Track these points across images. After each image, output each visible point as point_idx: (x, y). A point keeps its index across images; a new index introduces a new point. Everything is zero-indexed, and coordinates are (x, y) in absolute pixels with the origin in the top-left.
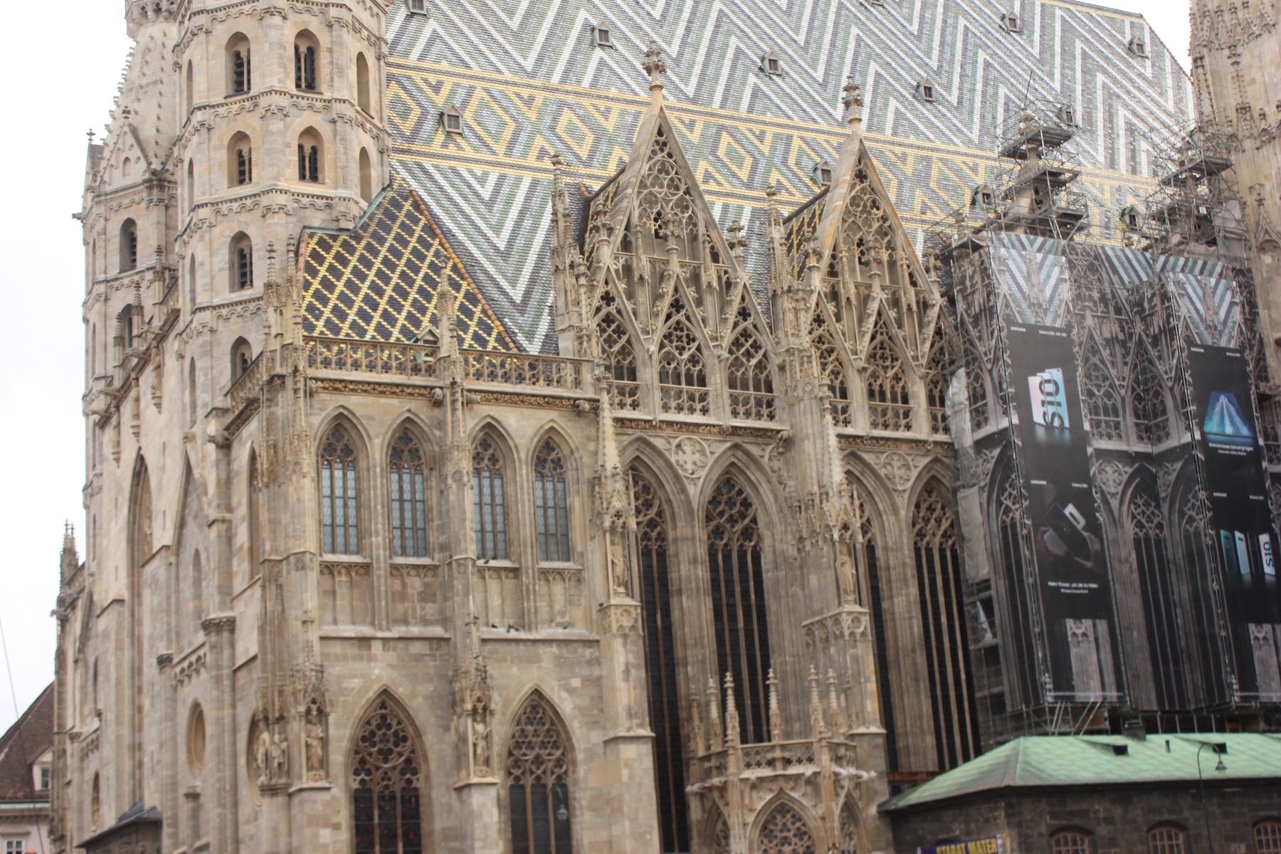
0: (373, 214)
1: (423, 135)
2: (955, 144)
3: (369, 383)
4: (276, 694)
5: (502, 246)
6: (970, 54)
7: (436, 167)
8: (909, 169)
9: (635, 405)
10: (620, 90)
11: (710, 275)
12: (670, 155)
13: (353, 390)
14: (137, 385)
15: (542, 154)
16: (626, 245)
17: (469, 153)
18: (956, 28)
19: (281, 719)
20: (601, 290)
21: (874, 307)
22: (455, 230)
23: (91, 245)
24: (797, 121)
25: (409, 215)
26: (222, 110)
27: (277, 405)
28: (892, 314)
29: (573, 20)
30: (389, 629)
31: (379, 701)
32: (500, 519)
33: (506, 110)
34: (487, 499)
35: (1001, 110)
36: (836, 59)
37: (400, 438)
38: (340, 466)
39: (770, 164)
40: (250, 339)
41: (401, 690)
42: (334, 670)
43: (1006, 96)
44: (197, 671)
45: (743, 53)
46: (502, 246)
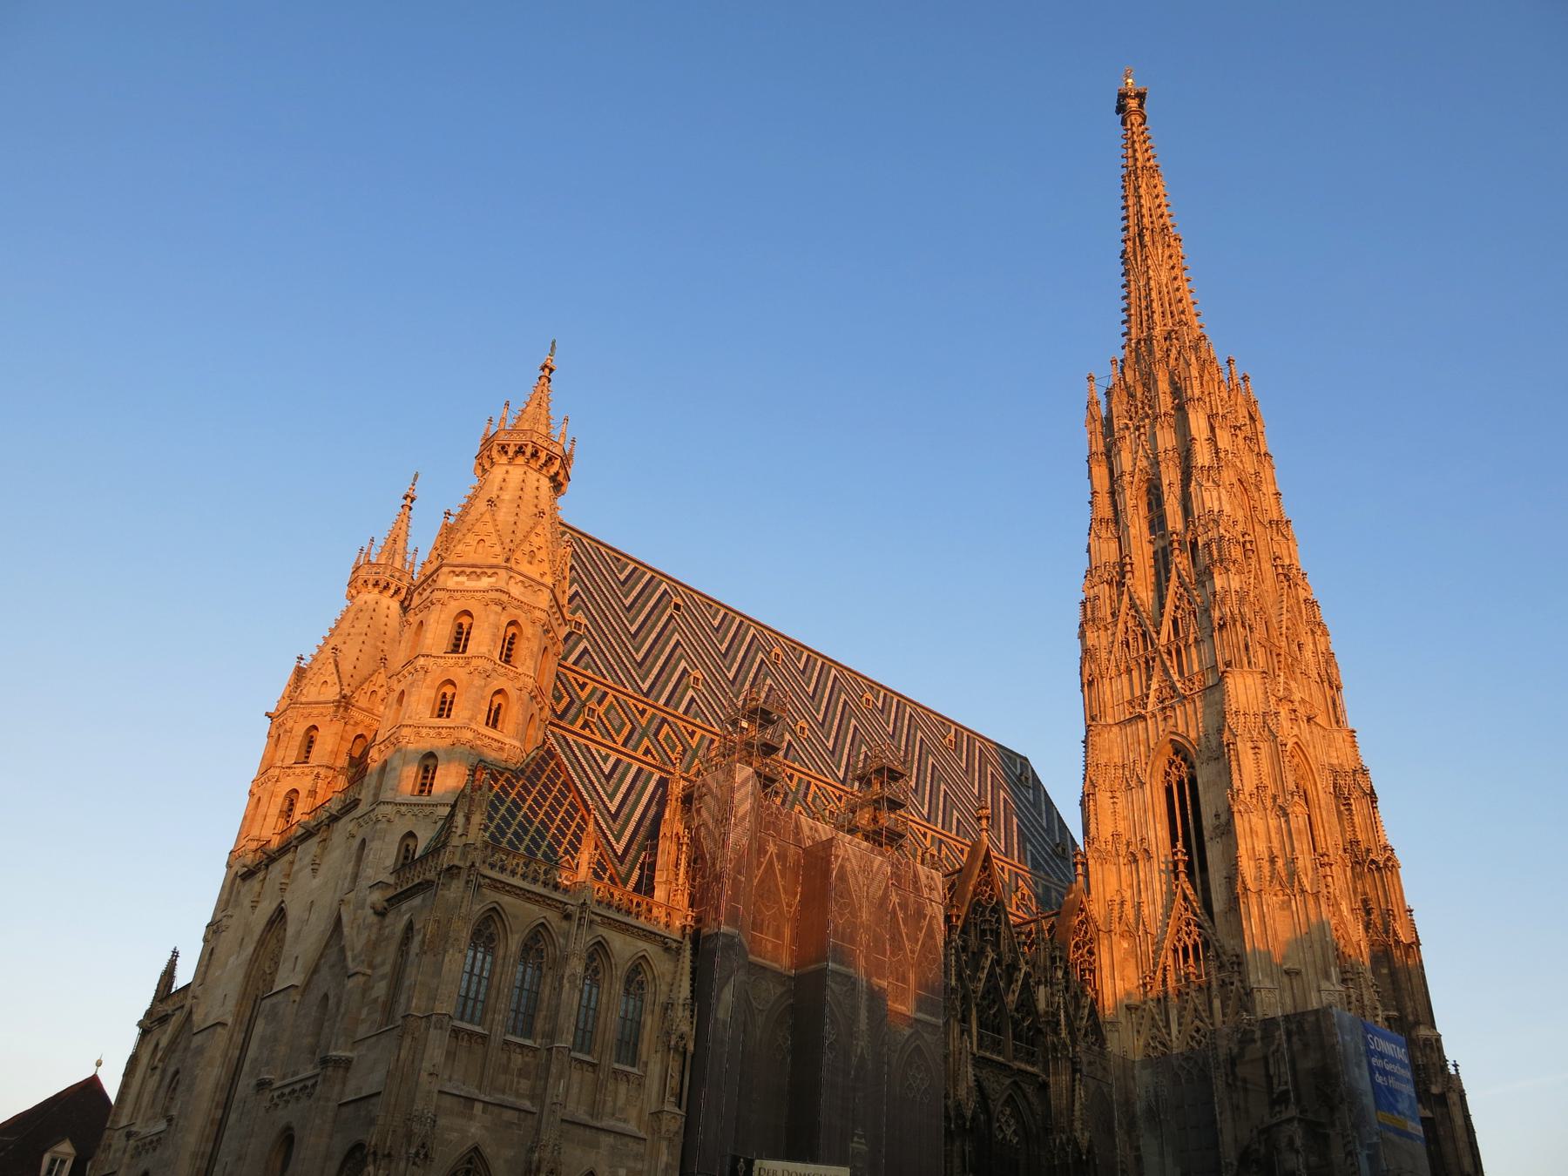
0: (528, 765)
3: (521, 889)
4: (390, 1133)
5: (613, 810)
7: (575, 741)
10: (703, 722)
13: (508, 891)
14: (295, 851)
15: (647, 752)
17: (598, 738)
19: (389, 1155)
22: (582, 790)
23: (275, 739)
24: (813, 773)
25: (553, 770)
26: (441, 661)
27: (449, 890)
29: (676, 666)
30: (490, 1095)
31: (468, 1156)
32: (590, 1020)
33: (627, 715)
34: (584, 1002)
35: (941, 799)
36: (841, 737)
37: (532, 938)
38: (482, 949)
40: (418, 835)
41: (488, 1150)
42: (442, 1122)
43: (945, 790)
44: (298, 1099)
46: (613, 810)
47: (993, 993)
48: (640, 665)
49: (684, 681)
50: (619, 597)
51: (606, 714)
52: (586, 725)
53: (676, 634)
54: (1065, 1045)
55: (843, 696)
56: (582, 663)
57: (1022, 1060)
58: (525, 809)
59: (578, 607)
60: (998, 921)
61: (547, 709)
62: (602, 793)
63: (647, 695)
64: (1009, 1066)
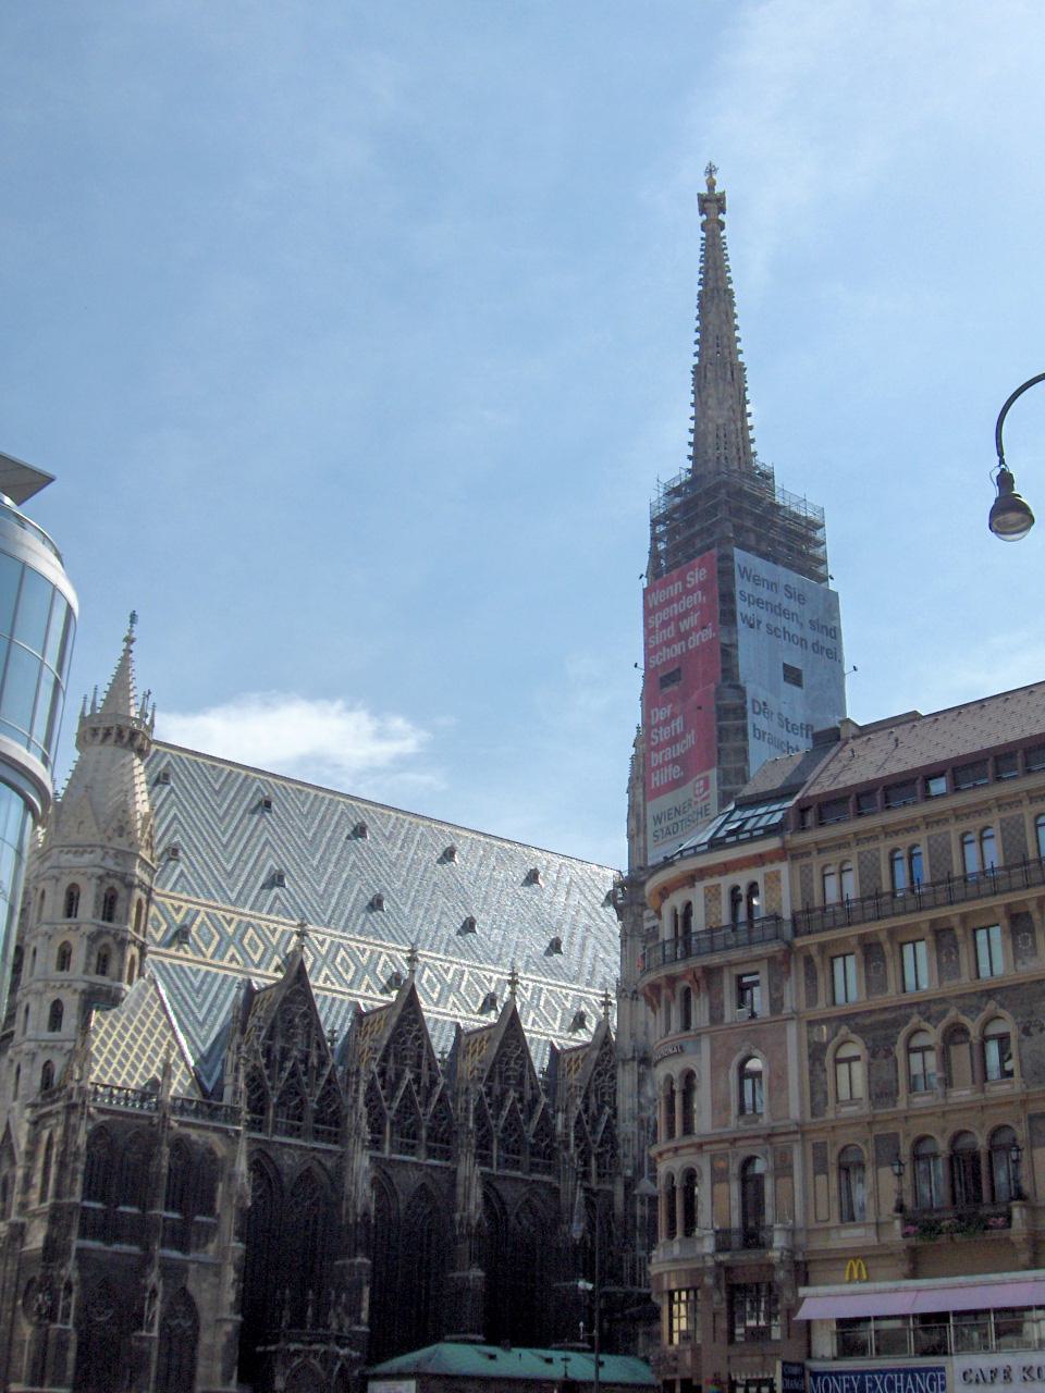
5: (201, 1018)
9: (260, 1130)
11: (314, 1060)
12: (303, 986)
15: (233, 958)
16: (270, 1036)
17: (190, 956)
20: (252, 1062)
21: (406, 1082)
26: (59, 927)
28: (415, 1088)
29: (263, 866)
46: (201, 1018)
47: (512, 1126)
50: (213, 809)
53: (266, 833)
54: (572, 1160)
56: (179, 888)
57: (539, 1172)
59: (176, 832)
60: (523, 1066)
62: (191, 1003)
64: (527, 1180)
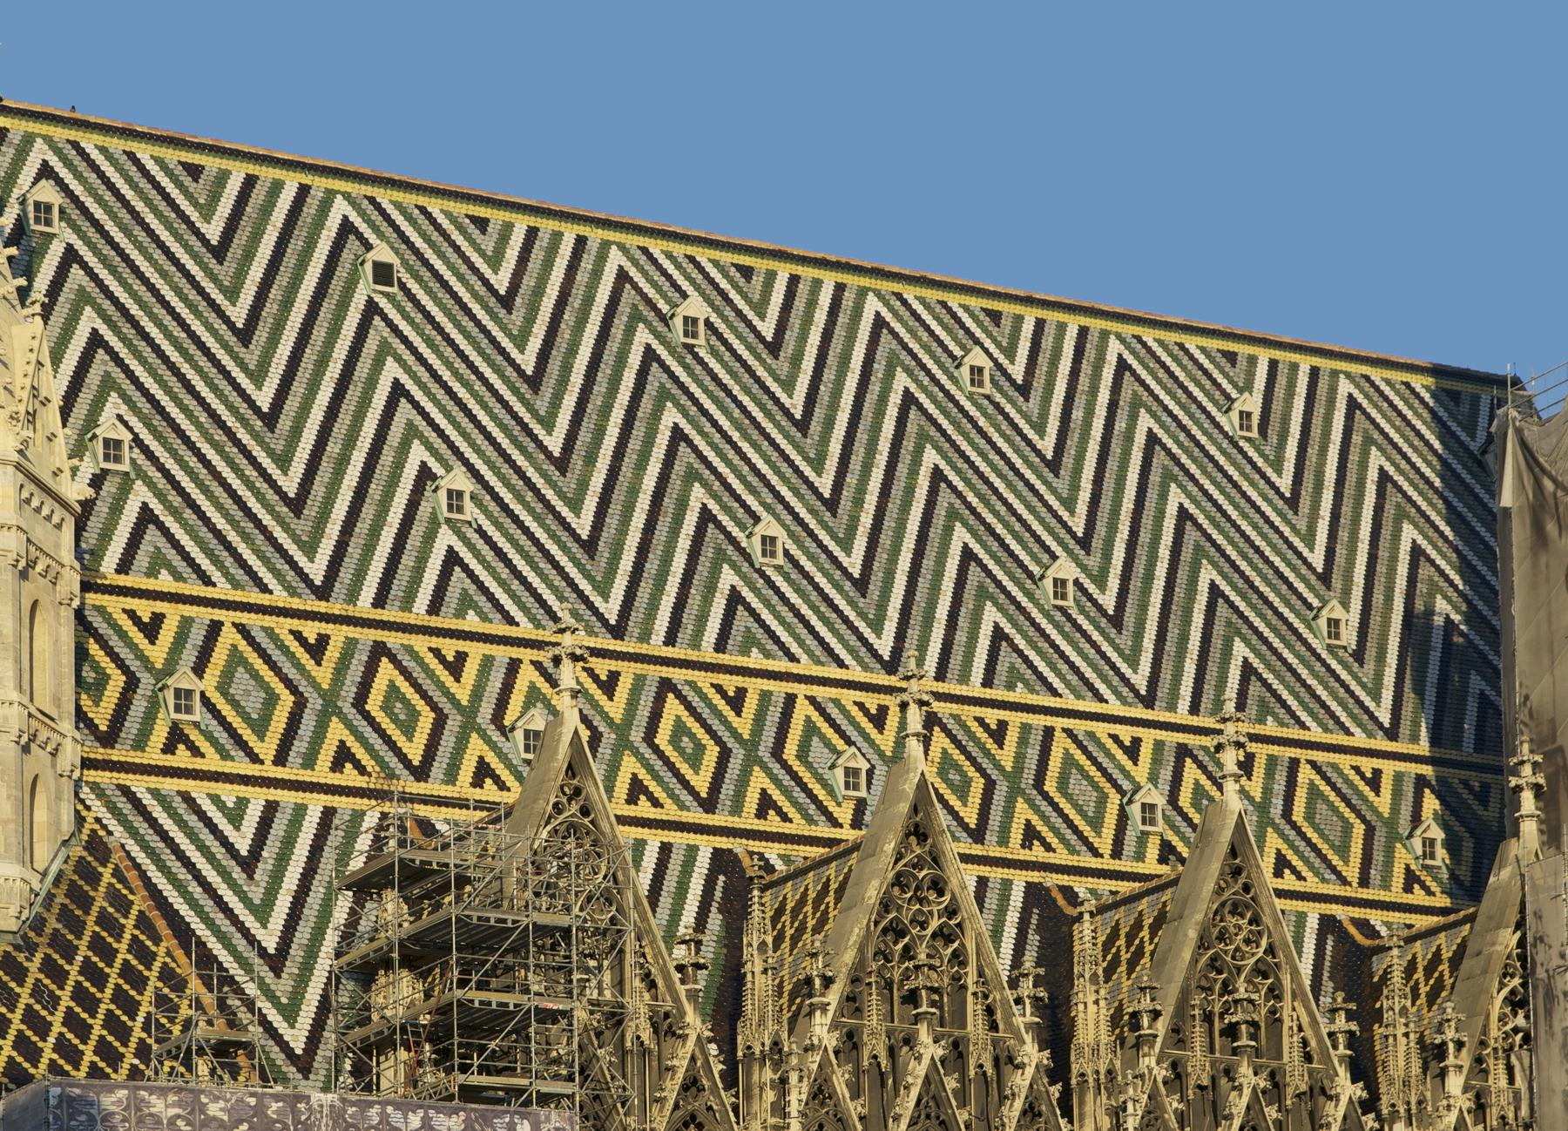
0: (50, 897)
1: (131, 726)
2: (1102, 700)
5: (271, 944)
6: (1152, 495)
7: (155, 793)
8: (1006, 757)
10: (484, 618)
15: (343, 756)
17: (212, 762)
18: (1129, 437)
24: (805, 667)
29: (399, 465)
35: (1198, 619)
36: (889, 523)
39: (751, 760)
43: (1213, 587)
45: (714, 519)
46: (271, 944)
48: (297, 505)
49: (424, 510)
51: (223, 689)
52: (176, 737)
55: (901, 381)
58: (57, 1028)
61: (68, 745)
63: (323, 592)
